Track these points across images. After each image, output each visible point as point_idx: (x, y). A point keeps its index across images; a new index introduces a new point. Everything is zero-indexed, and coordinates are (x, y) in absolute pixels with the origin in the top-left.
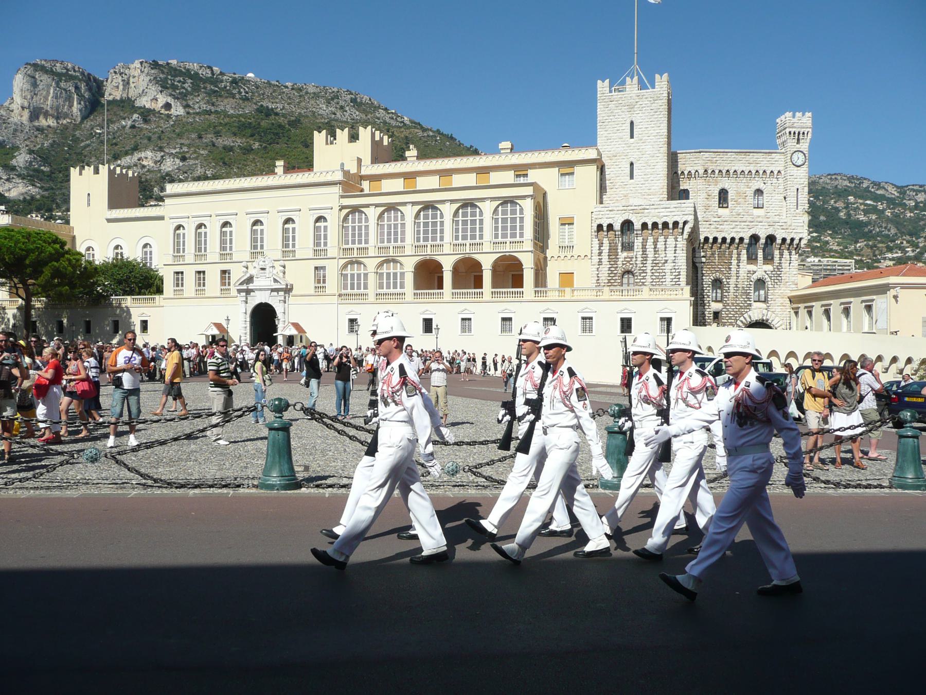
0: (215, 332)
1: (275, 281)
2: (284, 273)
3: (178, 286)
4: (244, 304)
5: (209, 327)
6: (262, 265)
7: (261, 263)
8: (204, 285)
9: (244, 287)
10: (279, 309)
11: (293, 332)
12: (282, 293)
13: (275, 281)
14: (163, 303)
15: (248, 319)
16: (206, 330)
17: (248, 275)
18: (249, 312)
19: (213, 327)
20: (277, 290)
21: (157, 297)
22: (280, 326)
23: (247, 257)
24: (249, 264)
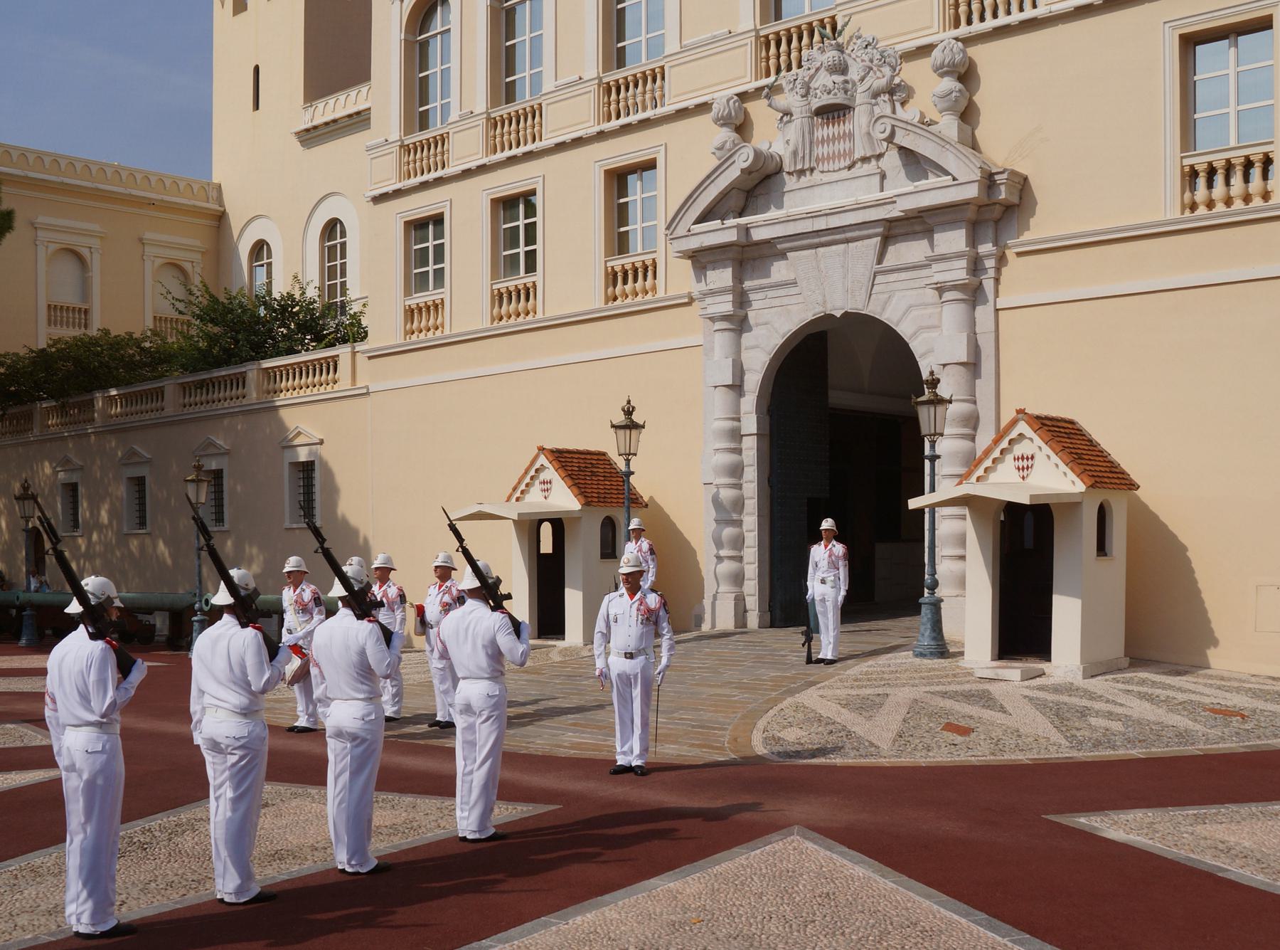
0: (564, 499)
1: (914, 162)
2: (968, 115)
3: (421, 282)
4: (722, 341)
5: (531, 475)
6: (825, 87)
7: (825, 79)
8: (531, 267)
9: (722, 232)
10: (935, 342)
11: (1052, 478)
12: (953, 240)
13: (914, 162)
14: (369, 375)
15: (750, 424)
16: (519, 491)
17: (744, 159)
18: (753, 381)
19: (551, 473)
20: (920, 223)
21: (343, 351)
22: (947, 448)
23: (735, 72)
24: (757, 109)
